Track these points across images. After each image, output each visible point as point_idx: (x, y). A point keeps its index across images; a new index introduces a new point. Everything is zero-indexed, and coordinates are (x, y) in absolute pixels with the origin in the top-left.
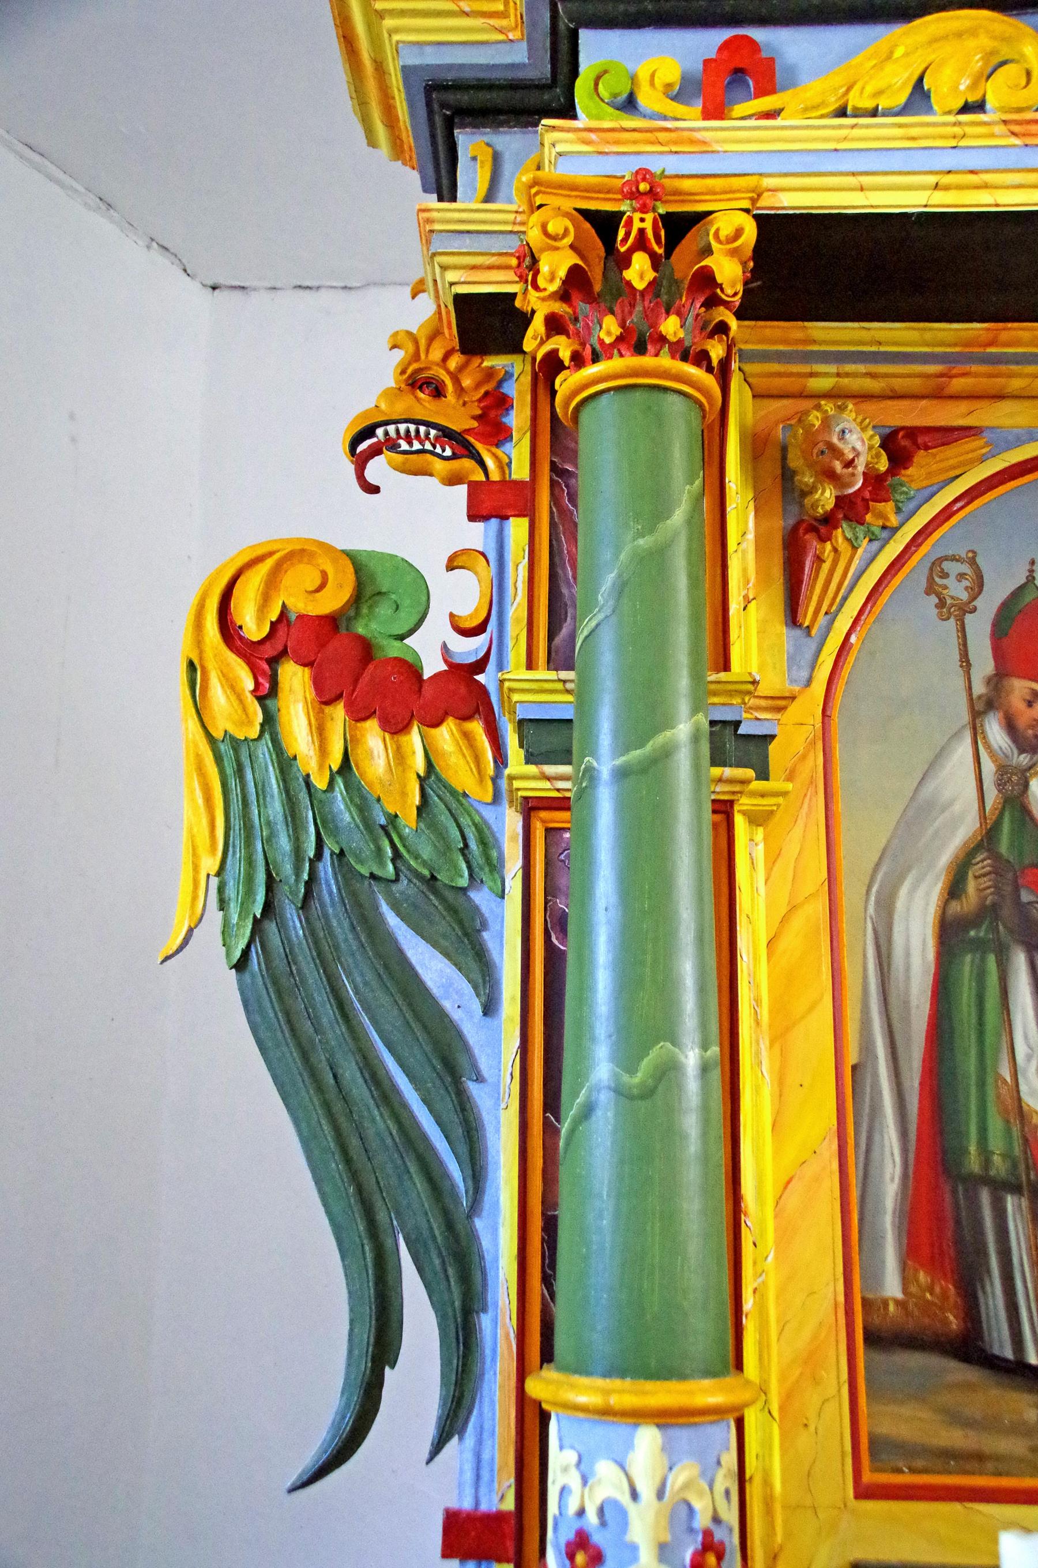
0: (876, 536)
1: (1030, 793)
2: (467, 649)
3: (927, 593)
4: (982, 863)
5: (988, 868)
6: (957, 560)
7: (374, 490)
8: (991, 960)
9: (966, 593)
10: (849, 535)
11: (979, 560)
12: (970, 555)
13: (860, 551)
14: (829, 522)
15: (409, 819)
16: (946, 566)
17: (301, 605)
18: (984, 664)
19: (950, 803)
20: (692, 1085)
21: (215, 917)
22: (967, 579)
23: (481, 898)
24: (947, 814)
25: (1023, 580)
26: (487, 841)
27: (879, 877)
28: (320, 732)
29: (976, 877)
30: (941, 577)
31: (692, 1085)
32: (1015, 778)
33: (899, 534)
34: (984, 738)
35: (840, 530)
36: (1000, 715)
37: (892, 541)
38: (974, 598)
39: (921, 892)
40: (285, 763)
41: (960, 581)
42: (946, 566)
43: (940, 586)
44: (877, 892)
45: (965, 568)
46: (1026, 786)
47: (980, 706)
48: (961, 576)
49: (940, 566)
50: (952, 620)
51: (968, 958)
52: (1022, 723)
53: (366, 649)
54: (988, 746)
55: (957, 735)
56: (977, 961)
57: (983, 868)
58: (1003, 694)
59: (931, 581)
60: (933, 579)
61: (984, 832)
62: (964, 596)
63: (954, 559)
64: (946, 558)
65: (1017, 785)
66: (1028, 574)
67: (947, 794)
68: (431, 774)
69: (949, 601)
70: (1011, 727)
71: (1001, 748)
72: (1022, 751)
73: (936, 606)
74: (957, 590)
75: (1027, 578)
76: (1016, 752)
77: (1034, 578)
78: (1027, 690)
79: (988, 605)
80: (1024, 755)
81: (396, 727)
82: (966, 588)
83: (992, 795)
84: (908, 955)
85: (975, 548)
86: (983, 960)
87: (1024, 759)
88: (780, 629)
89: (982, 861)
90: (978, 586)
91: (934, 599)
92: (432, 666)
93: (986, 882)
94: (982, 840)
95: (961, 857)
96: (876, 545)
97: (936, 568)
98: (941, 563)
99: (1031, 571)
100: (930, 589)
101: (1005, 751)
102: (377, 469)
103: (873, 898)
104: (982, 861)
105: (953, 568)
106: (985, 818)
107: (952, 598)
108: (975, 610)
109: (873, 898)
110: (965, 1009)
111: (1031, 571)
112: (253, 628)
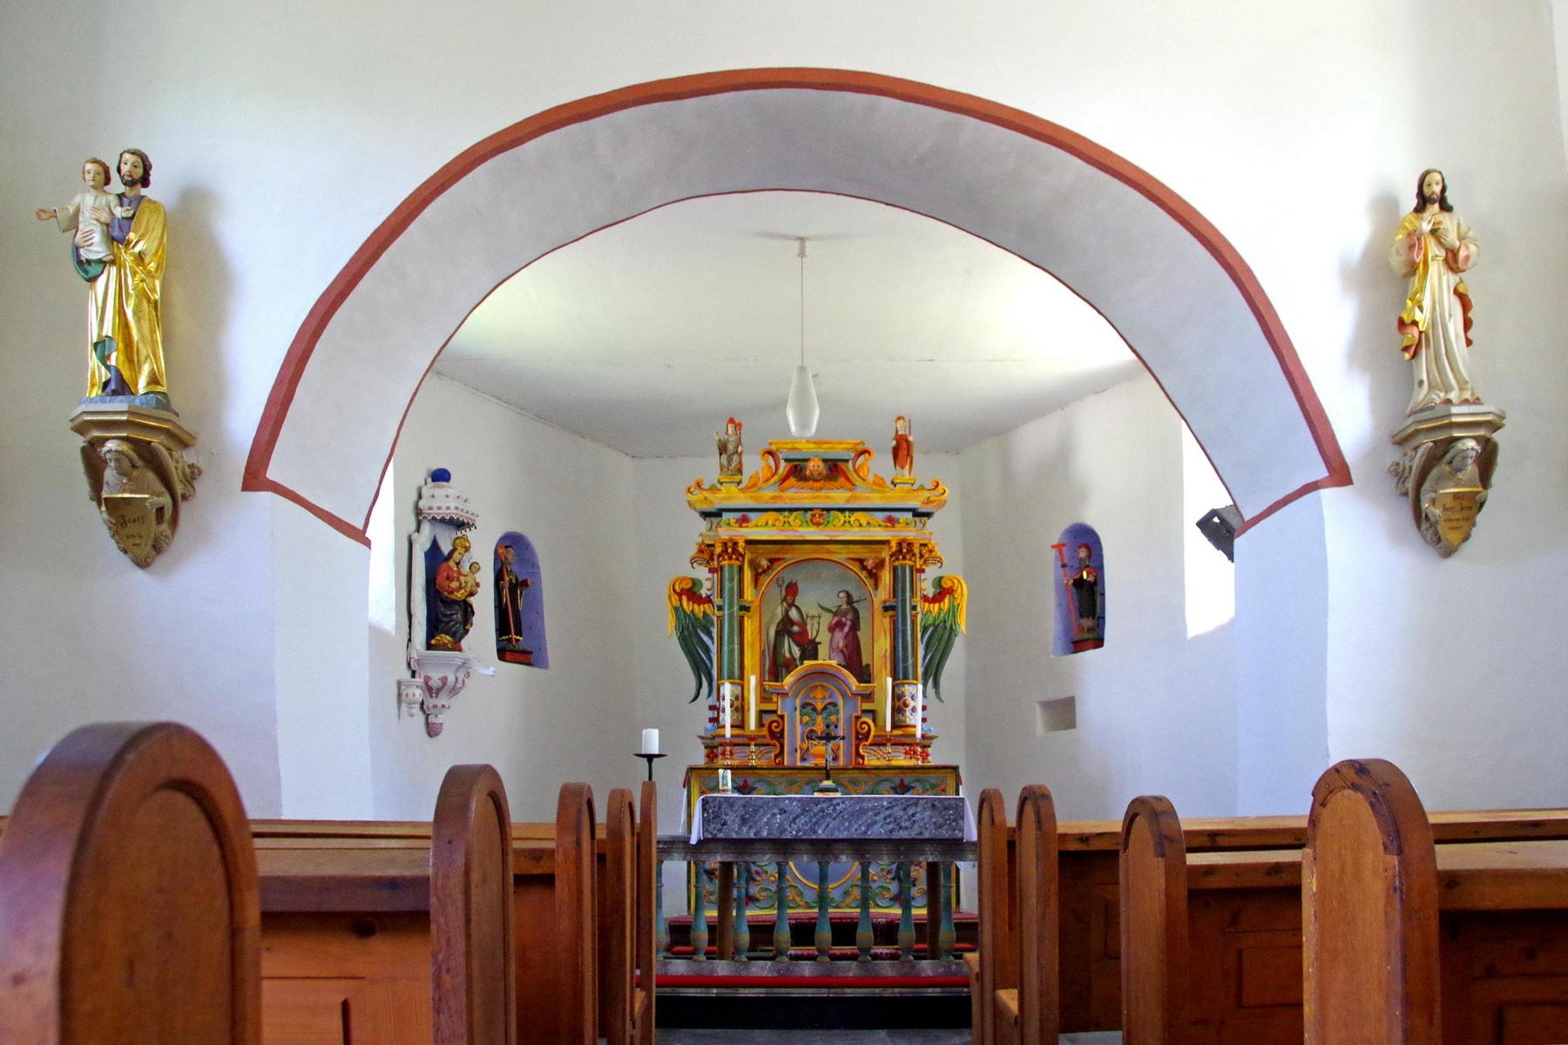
2: (709, 593)
7: (693, 568)
14: (761, 574)
15: (701, 618)
18: (784, 593)
21: (675, 632)
23: (712, 629)
26: (712, 620)
28: (688, 605)
40: (684, 610)
53: (695, 593)
68: (704, 613)
70: (787, 604)
81: (699, 605)
90: (784, 582)
92: (704, 596)
97: (778, 580)
102: (695, 565)
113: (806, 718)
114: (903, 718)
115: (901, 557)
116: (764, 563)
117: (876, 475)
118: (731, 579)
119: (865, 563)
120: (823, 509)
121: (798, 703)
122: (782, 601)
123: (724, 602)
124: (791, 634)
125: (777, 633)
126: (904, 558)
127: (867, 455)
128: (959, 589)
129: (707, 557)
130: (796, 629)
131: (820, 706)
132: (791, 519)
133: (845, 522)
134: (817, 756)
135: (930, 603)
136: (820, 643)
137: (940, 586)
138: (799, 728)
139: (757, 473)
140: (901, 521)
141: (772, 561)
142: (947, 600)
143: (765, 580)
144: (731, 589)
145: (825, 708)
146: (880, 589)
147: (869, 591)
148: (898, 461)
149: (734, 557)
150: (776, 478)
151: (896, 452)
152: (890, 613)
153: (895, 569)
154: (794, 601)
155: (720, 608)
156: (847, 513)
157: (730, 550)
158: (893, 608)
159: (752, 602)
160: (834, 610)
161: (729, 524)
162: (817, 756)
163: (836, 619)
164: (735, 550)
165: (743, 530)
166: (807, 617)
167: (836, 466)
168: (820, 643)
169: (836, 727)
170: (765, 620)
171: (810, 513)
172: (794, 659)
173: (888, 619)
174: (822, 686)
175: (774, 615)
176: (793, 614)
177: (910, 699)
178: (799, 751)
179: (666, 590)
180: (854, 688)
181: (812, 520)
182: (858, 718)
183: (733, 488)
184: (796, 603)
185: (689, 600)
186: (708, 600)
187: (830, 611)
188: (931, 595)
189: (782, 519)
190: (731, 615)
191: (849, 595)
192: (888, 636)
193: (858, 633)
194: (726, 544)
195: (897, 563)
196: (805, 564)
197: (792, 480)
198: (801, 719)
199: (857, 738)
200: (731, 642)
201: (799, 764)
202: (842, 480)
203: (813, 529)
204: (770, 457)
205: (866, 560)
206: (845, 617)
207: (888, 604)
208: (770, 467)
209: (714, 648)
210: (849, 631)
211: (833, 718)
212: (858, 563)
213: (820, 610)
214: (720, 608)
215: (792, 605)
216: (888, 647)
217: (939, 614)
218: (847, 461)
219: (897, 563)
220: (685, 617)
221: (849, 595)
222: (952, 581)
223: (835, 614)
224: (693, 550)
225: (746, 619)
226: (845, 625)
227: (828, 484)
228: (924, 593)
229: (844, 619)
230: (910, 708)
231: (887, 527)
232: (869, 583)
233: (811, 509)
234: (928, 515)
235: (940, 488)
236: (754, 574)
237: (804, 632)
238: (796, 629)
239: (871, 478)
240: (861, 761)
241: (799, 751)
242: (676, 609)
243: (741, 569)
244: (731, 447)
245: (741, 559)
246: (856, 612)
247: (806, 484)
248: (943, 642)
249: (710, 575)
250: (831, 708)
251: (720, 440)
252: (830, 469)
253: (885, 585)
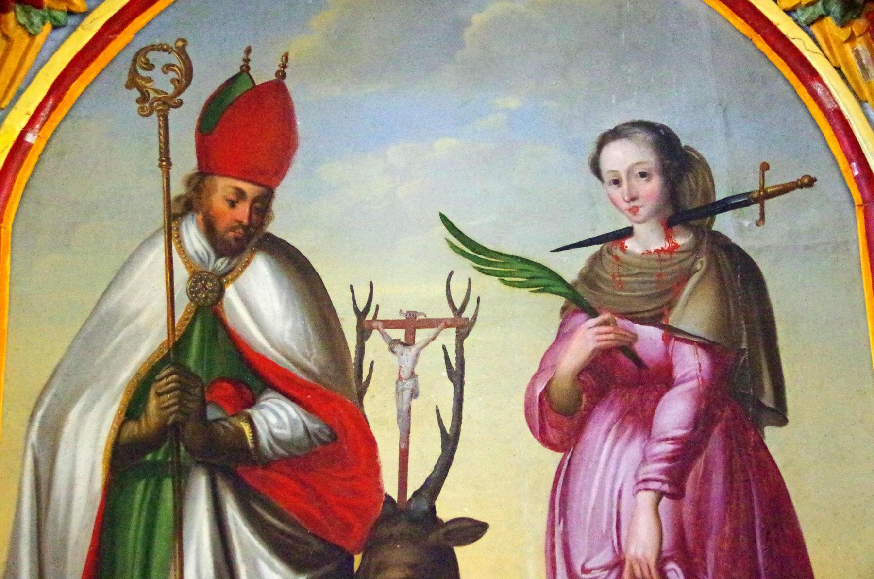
0: (59, 22)
1: (225, 300)
3: (128, 87)
4: (167, 379)
5: (173, 385)
6: (165, 50)
8: (168, 486)
9: (172, 85)
10: (23, 20)
11: (189, 50)
12: (180, 44)
13: (40, 39)
16: (152, 56)
19: (138, 314)
22: (174, 71)
24: (132, 327)
25: (237, 70)
27: (47, 400)
29: (159, 395)
30: (144, 69)
32: (209, 285)
33: (89, 19)
34: (180, 242)
35: (11, 15)
36: (199, 216)
37: (79, 29)
38: (179, 92)
39: (94, 415)
41: (165, 73)
42: (152, 56)
43: (143, 78)
44: (43, 417)
45: (174, 59)
46: (222, 291)
47: (177, 209)
48: (168, 67)
49: (144, 57)
50: (155, 116)
51: (141, 486)
52: (222, 226)
54: (182, 251)
55: (149, 240)
56: (151, 488)
57: (168, 383)
58: (204, 196)
59: (133, 73)
60: (136, 72)
61: (171, 345)
62: (170, 89)
63: (163, 48)
64: (153, 48)
65: (212, 291)
66: (242, 63)
67: (133, 305)
69: (152, 95)
70: (210, 230)
71: (196, 252)
72: (219, 255)
73: (138, 101)
75: (241, 67)
76: (213, 256)
77: (248, 68)
78: (231, 190)
80: (221, 260)
82: (173, 81)
83: (183, 303)
84: (71, 487)
85: (183, 37)
86: (159, 485)
87: (222, 264)
89: (167, 376)
91: (136, 94)
93: (169, 399)
94: (168, 354)
95: (143, 374)
96: (61, 33)
98: (147, 52)
99: (247, 60)
100: (133, 82)
101: (201, 256)
103: (36, 424)
104: (167, 376)
105: (158, 58)
106: (174, 330)
107: (156, 91)
108: (181, 103)
109: (36, 424)
110: (130, 544)
111: (247, 60)
147: (837, 118)
166: (364, 333)
184: (275, 228)
193: (772, 436)
206: (655, 320)
213: (465, 269)
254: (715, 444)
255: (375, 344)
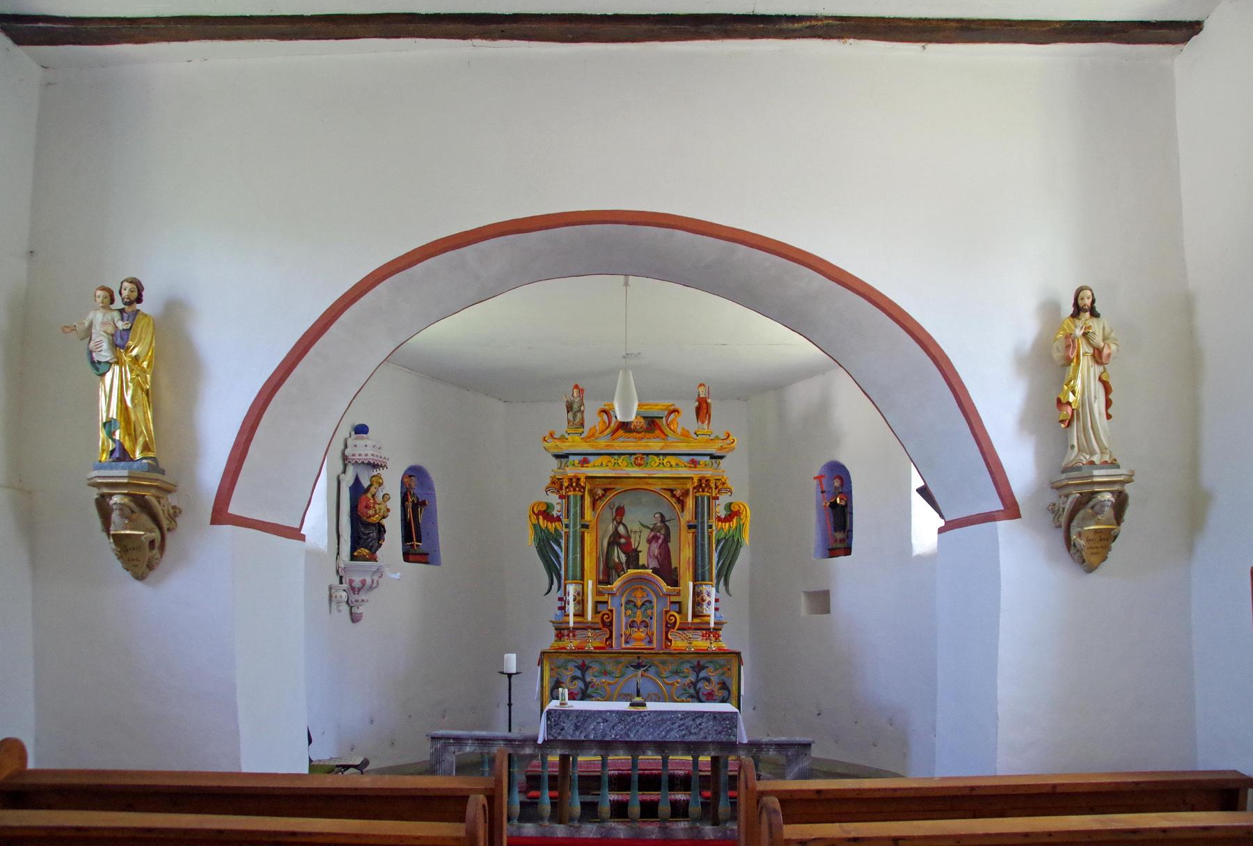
2: (559, 514)
14: (598, 500)
17: (541, 509)
18: (614, 514)
20: (578, 558)
23: (561, 540)
31: (578, 558)
40: (540, 527)
53: (548, 514)
68: (555, 528)
70: (617, 522)
74: (612, 506)
79: (615, 508)
81: (551, 522)
88: (592, 512)
90: (614, 506)
112: (536, 512)
113: (629, 612)
114: (701, 610)
115: (701, 490)
116: (600, 492)
117: (683, 429)
118: (575, 506)
119: (675, 493)
120: (644, 454)
121: (623, 600)
122: (613, 520)
123: (570, 521)
124: (619, 545)
125: (609, 544)
126: (703, 491)
127: (677, 413)
128: (744, 512)
129: (557, 486)
130: (623, 540)
131: (639, 603)
132: (620, 462)
133: (660, 463)
134: (636, 640)
135: (722, 522)
136: (641, 551)
137: (731, 510)
138: (624, 620)
139: (595, 426)
140: (701, 463)
141: (606, 490)
142: (735, 520)
143: (601, 504)
144: (575, 513)
145: (643, 605)
146: (685, 512)
148: (700, 419)
149: (577, 489)
150: (609, 430)
151: (698, 410)
152: (693, 530)
153: (696, 498)
154: (621, 519)
155: (567, 526)
156: (661, 457)
157: (574, 484)
158: (695, 527)
159: (590, 521)
160: (651, 527)
161: (574, 465)
162: (636, 640)
163: (652, 534)
164: (578, 484)
165: (584, 469)
167: (653, 422)
168: (641, 551)
169: (651, 618)
170: (600, 533)
171: (634, 457)
172: (622, 563)
173: (691, 534)
174: (642, 589)
175: (606, 531)
176: (621, 529)
177: (706, 596)
178: (624, 636)
179: (528, 512)
180: (665, 590)
181: (635, 462)
182: (667, 612)
183: (577, 438)
185: (544, 519)
186: (558, 519)
187: (648, 527)
188: (723, 516)
189: (613, 461)
190: (575, 532)
191: (662, 516)
192: (691, 547)
194: (571, 479)
195: (698, 494)
196: (633, 492)
197: (621, 432)
198: (625, 613)
199: (667, 626)
200: (575, 553)
201: (624, 646)
202: (658, 432)
203: (636, 469)
204: (605, 415)
205: (675, 490)
207: (691, 524)
208: (604, 422)
209: (562, 555)
210: (663, 542)
211: (649, 612)
212: (669, 493)
214: (567, 526)
215: (620, 523)
216: (691, 556)
217: (729, 531)
218: (662, 418)
219: (698, 494)
220: (541, 532)
221: (662, 516)
222: (739, 507)
223: (652, 530)
224: (548, 481)
225: (586, 534)
226: (659, 538)
227: (648, 435)
228: (719, 515)
229: (658, 534)
230: (706, 602)
231: (690, 467)
232: (677, 507)
233: (634, 454)
234: (721, 457)
235: (731, 438)
236: (592, 499)
237: (629, 543)
238: (623, 540)
239: (679, 431)
240: (670, 644)
241: (624, 636)
242: (534, 526)
243: (582, 497)
244: (576, 406)
245: (582, 490)
246: (667, 528)
247: (632, 435)
248: (732, 551)
249: (560, 501)
250: (648, 604)
251: (568, 401)
252: (649, 424)
253: (689, 508)
254: (664, 545)
255: (632, 534)
